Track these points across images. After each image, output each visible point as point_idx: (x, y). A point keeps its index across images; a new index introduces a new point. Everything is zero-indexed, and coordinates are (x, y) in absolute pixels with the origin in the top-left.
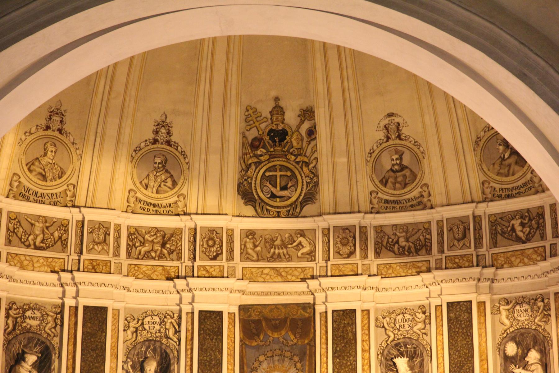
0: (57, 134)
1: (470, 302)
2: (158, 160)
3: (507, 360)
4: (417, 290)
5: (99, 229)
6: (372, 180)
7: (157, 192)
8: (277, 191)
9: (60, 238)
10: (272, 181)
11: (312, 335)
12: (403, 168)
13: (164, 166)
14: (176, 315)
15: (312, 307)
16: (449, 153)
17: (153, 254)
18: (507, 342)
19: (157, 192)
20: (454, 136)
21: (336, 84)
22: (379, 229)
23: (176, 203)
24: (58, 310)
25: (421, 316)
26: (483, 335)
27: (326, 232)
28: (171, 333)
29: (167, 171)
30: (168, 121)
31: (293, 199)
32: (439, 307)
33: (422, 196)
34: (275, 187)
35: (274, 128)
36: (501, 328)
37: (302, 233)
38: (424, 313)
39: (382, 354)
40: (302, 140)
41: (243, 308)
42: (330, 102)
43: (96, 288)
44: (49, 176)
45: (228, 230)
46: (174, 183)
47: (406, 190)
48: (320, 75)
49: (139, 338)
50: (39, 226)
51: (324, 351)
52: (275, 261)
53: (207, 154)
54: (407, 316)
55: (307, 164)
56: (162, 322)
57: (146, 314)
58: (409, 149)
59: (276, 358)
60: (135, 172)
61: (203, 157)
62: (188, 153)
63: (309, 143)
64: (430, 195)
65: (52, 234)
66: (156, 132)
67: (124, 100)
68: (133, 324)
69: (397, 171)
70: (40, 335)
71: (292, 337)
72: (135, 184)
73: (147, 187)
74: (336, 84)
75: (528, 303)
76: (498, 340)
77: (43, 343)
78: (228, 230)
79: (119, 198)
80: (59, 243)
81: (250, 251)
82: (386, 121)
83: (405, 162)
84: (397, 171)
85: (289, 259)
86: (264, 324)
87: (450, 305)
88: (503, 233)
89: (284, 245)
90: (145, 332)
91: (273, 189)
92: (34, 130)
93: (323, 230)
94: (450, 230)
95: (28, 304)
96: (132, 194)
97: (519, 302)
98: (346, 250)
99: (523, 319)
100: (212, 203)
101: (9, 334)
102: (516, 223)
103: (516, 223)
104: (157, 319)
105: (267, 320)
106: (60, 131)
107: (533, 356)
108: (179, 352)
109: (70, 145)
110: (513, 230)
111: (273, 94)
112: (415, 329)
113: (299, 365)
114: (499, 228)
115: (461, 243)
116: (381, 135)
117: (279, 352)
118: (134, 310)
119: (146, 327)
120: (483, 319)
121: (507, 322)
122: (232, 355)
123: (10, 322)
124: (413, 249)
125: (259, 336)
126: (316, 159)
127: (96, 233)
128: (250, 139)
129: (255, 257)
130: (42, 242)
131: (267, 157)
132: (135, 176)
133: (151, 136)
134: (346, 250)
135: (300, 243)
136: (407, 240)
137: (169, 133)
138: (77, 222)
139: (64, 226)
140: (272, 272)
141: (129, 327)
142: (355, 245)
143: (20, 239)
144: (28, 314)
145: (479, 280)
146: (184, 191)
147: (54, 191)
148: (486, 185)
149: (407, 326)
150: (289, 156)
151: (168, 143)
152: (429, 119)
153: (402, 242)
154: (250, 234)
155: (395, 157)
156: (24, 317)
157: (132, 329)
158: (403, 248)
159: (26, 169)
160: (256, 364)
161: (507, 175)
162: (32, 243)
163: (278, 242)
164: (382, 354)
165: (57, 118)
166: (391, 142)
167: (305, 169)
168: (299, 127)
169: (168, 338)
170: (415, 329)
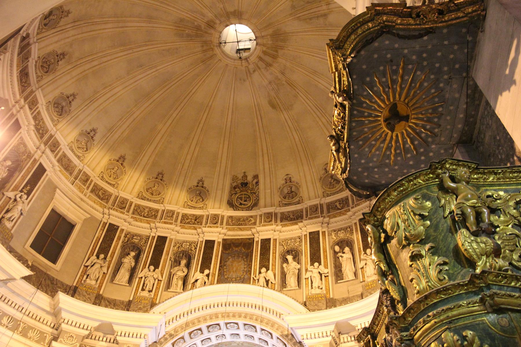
0: (160, 180)
1: (319, 231)
2: (198, 192)
3: (335, 253)
4: (297, 231)
5: (170, 212)
6: (280, 197)
7: (196, 203)
8: (243, 202)
9: (154, 215)
10: (241, 199)
11: (252, 249)
12: (292, 192)
13: (200, 194)
14: (196, 243)
16: (310, 184)
17: (191, 223)
18: (335, 245)
19: (196, 203)
20: (311, 178)
21: (267, 166)
22: (282, 214)
23: (203, 207)
24: (148, 238)
25: (298, 240)
26: (325, 243)
27: (261, 216)
28: (193, 249)
29: (201, 196)
30: (203, 180)
31: (249, 205)
32: (305, 235)
33: (300, 201)
34: (242, 200)
35: (243, 181)
36: (332, 241)
37: (252, 217)
38: (300, 239)
39: (281, 255)
40: (254, 185)
41: (224, 240)
42: (264, 172)
43: (164, 230)
44: (154, 194)
45: (222, 216)
46: (203, 200)
47: (293, 199)
48: (261, 164)
49: (179, 249)
50: (147, 210)
51: (256, 254)
52: (240, 225)
53: (216, 190)
54: (293, 241)
55: (255, 193)
56: (190, 245)
57: (184, 242)
58: (295, 185)
59: (236, 257)
60: (188, 196)
61: (215, 191)
62: (209, 190)
63: (256, 186)
64: (302, 200)
65: (152, 213)
66: (198, 183)
67: (187, 172)
69: (290, 193)
70: (138, 245)
71: (243, 250)
72: (188, 200)
73: (192, 201)
74: (267, 166)
75: (344, 230)
76: (331, 244)
77: (139, 248)
78: (222, 216)
79: (181, 203)
80: (154, 216)
81: (230, 223)
82: (286, 177)
83: (293, 190)
84: (290, 193)
85: (246, 225)
86: (232, 245)
87: (310, 233)
88: (332, 208)
89: (244, 220)
91: (241, 201)
92: (151, 178)
93: (260, 215)
94: (310, 209)
95: (136, 234)
96: (186, 203)
97: (340, 230)
98: (269, 220)
99: (341, 236)
100: (217, 205)
101: (124, 243)
102: (337, 204)
103: (337, 204)
104: (188, 244)
105: (233, 243)
106: (161, 180)
107: (347, 249)
108: (195, 255)
109: (164, 185)
110: (336, 206)
111: (243, 171)
112: (296, 245)
113: (245, 260)
114: (330, 207)
115: (315, 213)
116: (284, 182)
117: (237, 255)
118: (179, 240)
119: (183, 246)
120: (324, 237)
121: (335, 238)
122: (217, 256)
123: (126, 239)
124: (296, 218)
125: (229, 249)
126: (259, 192)
127: (169, 213)
128: (233, 186)
129: (232, 224)
130: (147, 215)
131: (239, 191)
132: (188, 197)
133: (196, 184)
134: (269, 220)
135: (250, 220)
136: (293, 216)
137: (203, 184)
138: (162, 210)
139: (157, 211)
140: (238, 229)
142: (272, 218)
143: (138, 213)
144: (135, 237)
145: (322, 223)
146: (206, 203)
147: (155, 199)
148: (325, 193)
150: (248, 191)
151: (202, 187)
152: (302, 174)
153: (291, 217)
154: (231, 217)
155: (289, 189)
156: (133, 238)
157: (177, 246)
158: (292, 218)
159: (146, 191)
160: (227, 260)
161: (333, 188)
162: (143, 215)
163: (242, 220)
164: (281, 255)
165: (161, 176)
166: (287, 184)
167: (254, 195)
168: (252, 181)
169: (191, 250)
170: (296, 245)
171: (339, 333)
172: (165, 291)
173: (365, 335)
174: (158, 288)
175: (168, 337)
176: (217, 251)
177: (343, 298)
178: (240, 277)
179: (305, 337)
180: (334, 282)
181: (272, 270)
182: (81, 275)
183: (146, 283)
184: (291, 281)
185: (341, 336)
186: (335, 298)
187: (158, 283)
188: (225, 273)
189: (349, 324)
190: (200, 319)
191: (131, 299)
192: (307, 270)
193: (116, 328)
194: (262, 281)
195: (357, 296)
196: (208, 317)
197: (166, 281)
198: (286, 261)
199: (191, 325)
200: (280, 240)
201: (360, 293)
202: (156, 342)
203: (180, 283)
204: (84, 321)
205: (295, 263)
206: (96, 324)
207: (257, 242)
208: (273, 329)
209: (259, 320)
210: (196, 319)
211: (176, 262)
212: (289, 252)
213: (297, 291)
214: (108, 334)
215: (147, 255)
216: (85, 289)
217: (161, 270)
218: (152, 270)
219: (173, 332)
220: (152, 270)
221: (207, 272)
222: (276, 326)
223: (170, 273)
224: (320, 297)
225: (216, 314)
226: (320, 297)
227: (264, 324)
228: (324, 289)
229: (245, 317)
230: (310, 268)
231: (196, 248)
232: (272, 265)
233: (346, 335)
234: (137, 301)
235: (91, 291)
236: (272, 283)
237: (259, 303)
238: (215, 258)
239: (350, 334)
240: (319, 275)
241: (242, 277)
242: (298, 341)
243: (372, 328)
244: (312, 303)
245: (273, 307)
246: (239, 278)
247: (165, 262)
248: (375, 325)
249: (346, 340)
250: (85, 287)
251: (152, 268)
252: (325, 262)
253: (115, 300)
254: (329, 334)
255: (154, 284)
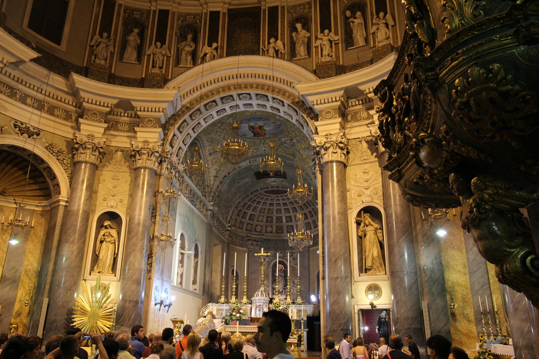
3: (347, 18)
14: (200, 15)
15: (260, 7)
18: (346, 10)
25: (307, 6)
38: (309, 4)
39: (290, 23)
41: (229, 10)
49: (184, 24)
54: (301, 7)
56: (194, 18)
57: (187, 14)
68: (181, 18)
90: (186, 22)
104: (192, 17)
107: (359, 14)
108: (201, 28)
112: (305, 11)
113: (253, 30)
119: (187, 19)
122: (223, 28)
123: (126, 15)
141: (180, 19)
144: (135, 12)
149: (301, 11)
156: (133, 14)
157: (181, 20)
164: (290, 23)
169: (196, 23)
170: (305, 11)
171: (348, 98)
172: (175, 67)
173: (382, 87)
174: (168, 65)
175: (185, 110)
176: (223, 23)
177: (353, 65)
178: (249, 49)
179: (315, 103)
180: (344, 49)
181: (281, 40)
182: (89, 56)
183: (155, 59)
184: (301, 50)
185: (350, 101)
186: (345, 64)
187: (167, 59)
188: (234, 46)
189: (358, 89)
190: (213, 92)
191: (144, 76)
192: (316, 38)
193: (134, 104)
194: (271, 51)
195: (366, 62)
196: (221, 90)
197: (175, 57)
198: (294, 29)
199: (205, 97)
200: (288, 7)
201: (370, 59)
202: (174, 115)
203: (189, 58)
204: (103, 100)
205: (304, 31)
206: (115, 101)
207: (265, 10)
208: (284, 98)
209: (271, 90)
210: (210, 92)
211: (182, 37)
212: (297, 20)
213: (307, 59)
214: (128, 110)
215: (151, 31)
216: (96, 69)
217: (169, 46)
218: (159, 47)
219: (188, 105)
220: (159, 47)
221: (215, 45)
222: (287, 94)
223: (178, 48)
224: (330, 65)
225: (228, 86)
226: (330, 65)
227: (276, 93)
228: (334, 56)
229: (257, 88)
230: (320, 36)
231: (201, 21)
232: (281, 34)
233: (355, 100)
234: (150, 78)
235: (103, 70)
236: (281, 53)
237: (270, 73)
238: (222, 31)
239: (358, 99)
240: (329, 42)
241: (251, 48)
242: (308, 107)
243: (390, 80)
244: (322, 71)
245: (284, 77)
246: (248, 50)
247: (171, 37)
248: (393, 77)
249: (354, 104)
250: (96, 67)
251: (159, 44)
252: (335, 29)
253: (128, 78)
254: (338, 99)
255: (163, 61)
